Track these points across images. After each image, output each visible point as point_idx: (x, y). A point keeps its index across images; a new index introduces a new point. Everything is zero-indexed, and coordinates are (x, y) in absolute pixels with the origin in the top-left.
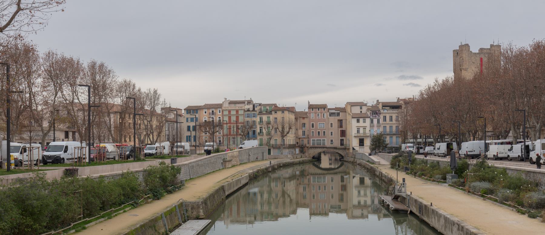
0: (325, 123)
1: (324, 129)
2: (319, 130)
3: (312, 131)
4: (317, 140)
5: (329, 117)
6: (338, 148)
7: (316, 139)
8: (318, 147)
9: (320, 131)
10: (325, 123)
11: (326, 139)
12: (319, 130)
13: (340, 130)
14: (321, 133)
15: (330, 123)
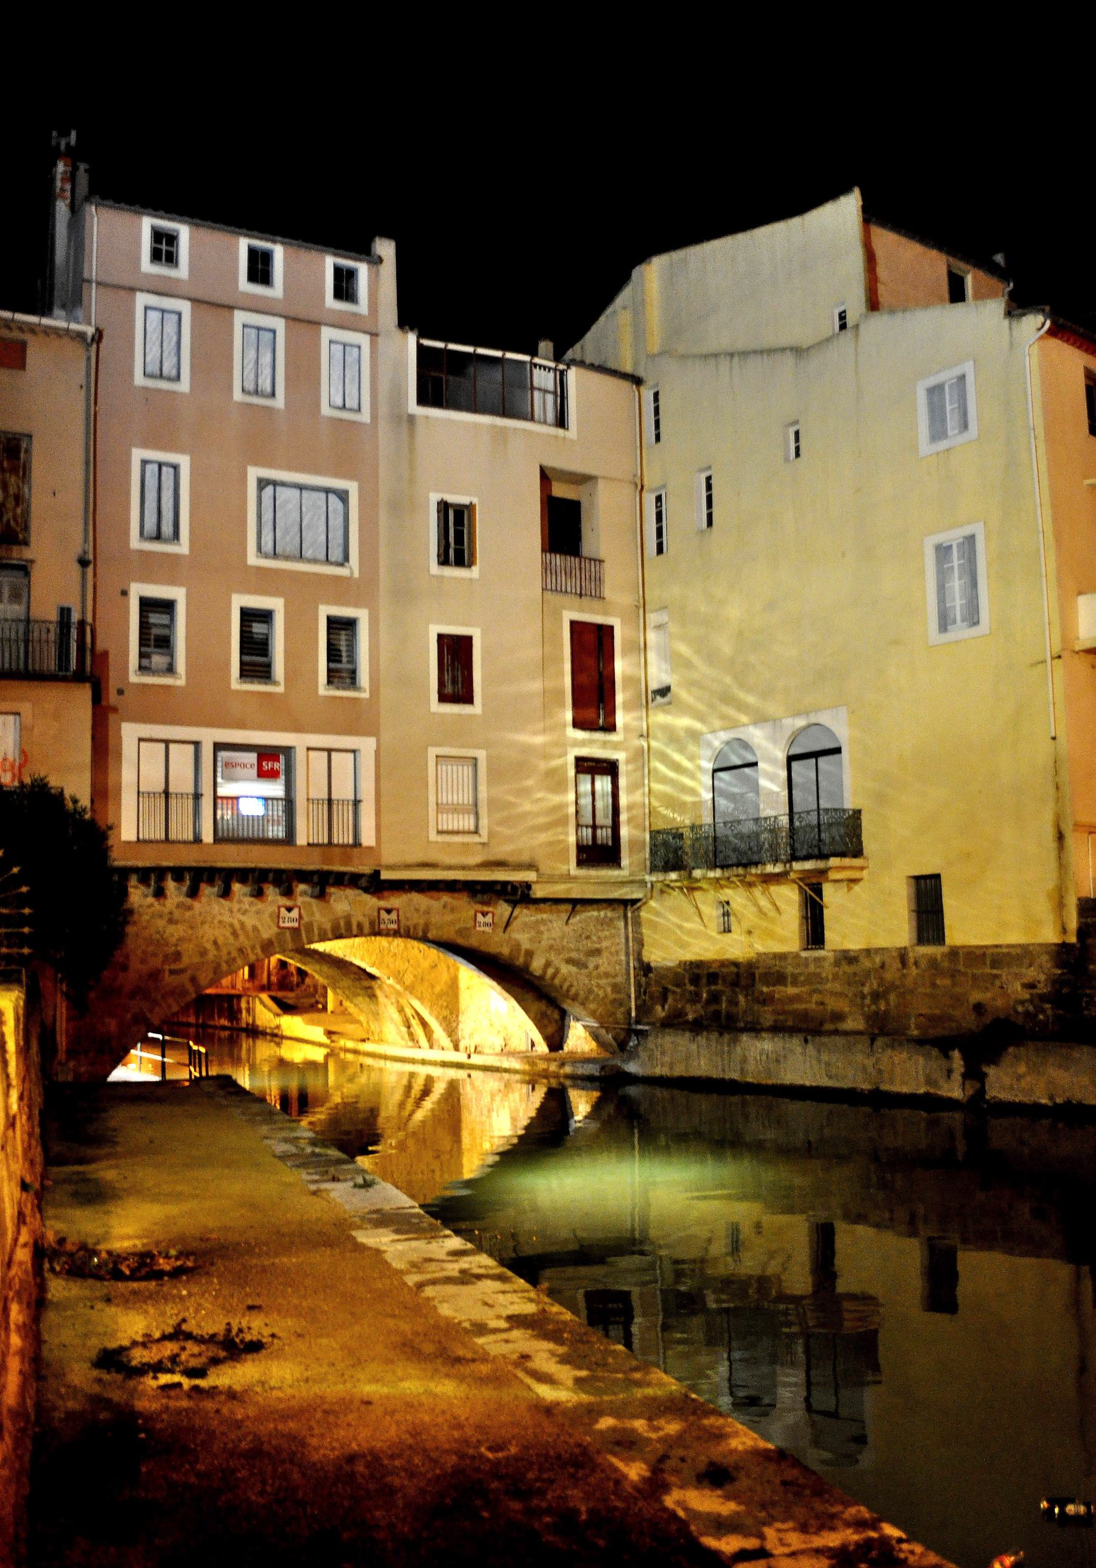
0: (352, 488)
1: (340, 589)
2: (264, 581)
3: (138, 590)
4: (218, 747)
5: (413, 406)
6: (538, 892)
7: (209, 736)
8: (243, 875)
9: (275, 604)
10: (352, 488)
11: (367, 745)
12: (264, 581)
13: (574, 624)
14: (297, 656)
15: (434, 498)
